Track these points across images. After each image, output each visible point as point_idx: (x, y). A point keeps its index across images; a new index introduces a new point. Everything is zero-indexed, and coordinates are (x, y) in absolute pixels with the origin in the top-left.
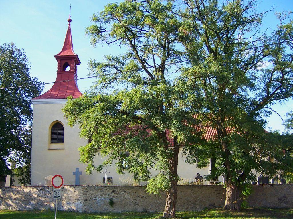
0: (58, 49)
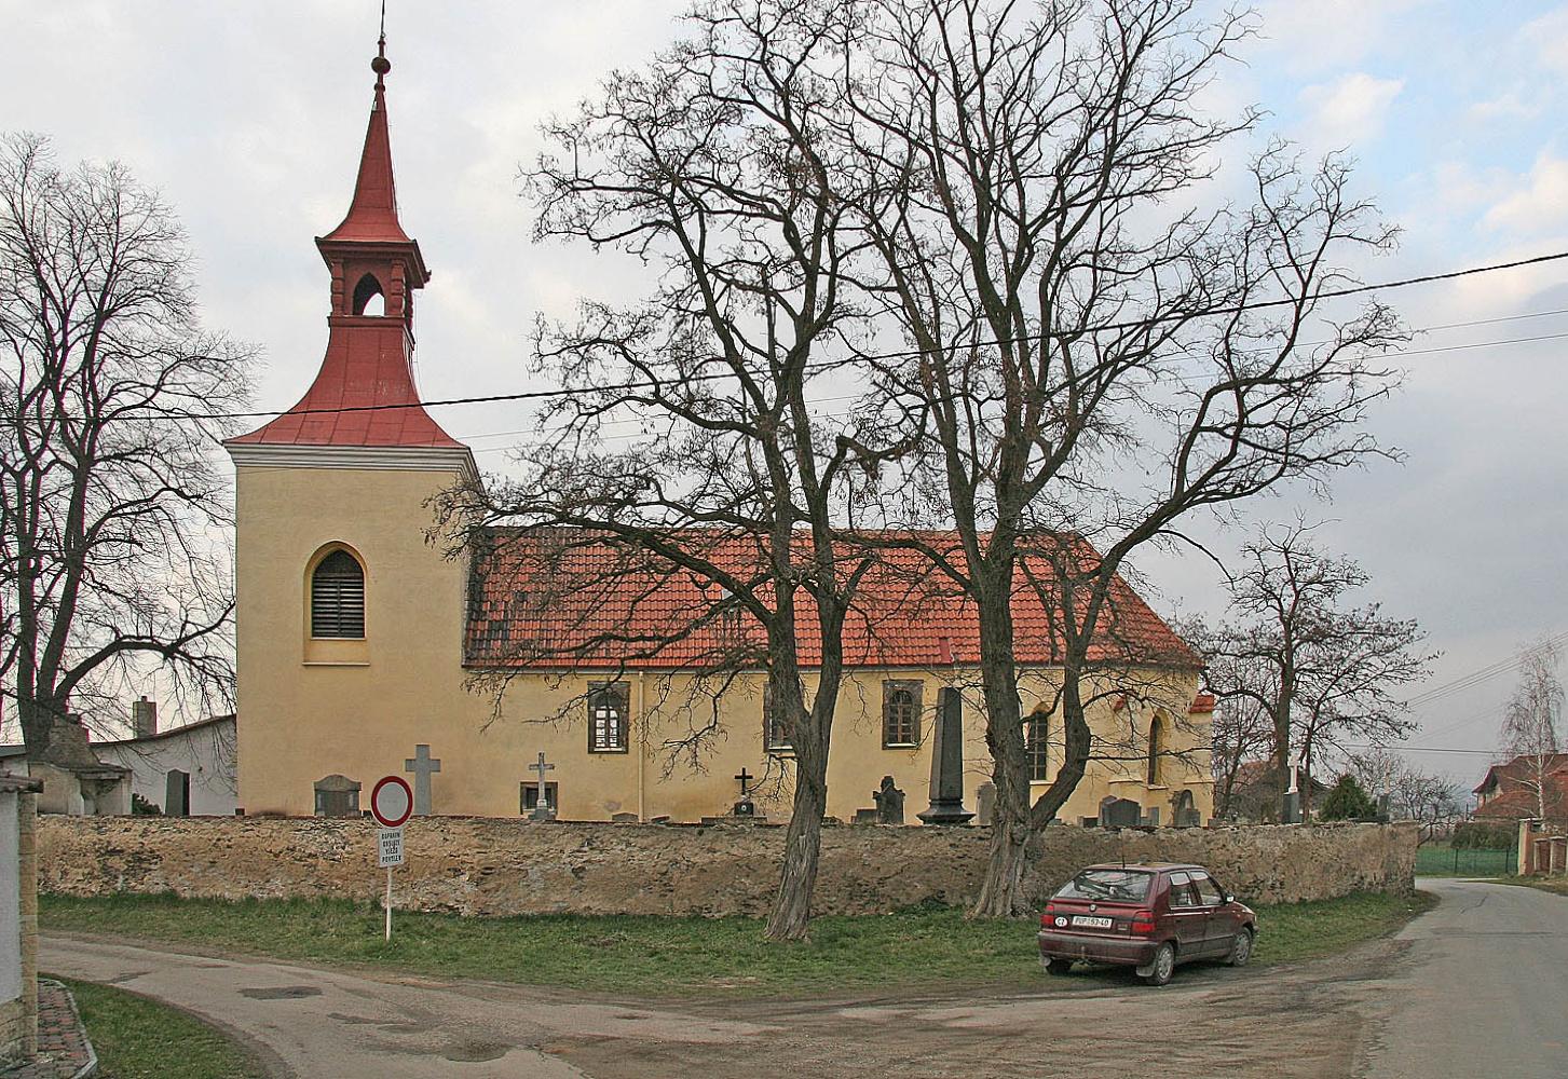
0: (331, 211)
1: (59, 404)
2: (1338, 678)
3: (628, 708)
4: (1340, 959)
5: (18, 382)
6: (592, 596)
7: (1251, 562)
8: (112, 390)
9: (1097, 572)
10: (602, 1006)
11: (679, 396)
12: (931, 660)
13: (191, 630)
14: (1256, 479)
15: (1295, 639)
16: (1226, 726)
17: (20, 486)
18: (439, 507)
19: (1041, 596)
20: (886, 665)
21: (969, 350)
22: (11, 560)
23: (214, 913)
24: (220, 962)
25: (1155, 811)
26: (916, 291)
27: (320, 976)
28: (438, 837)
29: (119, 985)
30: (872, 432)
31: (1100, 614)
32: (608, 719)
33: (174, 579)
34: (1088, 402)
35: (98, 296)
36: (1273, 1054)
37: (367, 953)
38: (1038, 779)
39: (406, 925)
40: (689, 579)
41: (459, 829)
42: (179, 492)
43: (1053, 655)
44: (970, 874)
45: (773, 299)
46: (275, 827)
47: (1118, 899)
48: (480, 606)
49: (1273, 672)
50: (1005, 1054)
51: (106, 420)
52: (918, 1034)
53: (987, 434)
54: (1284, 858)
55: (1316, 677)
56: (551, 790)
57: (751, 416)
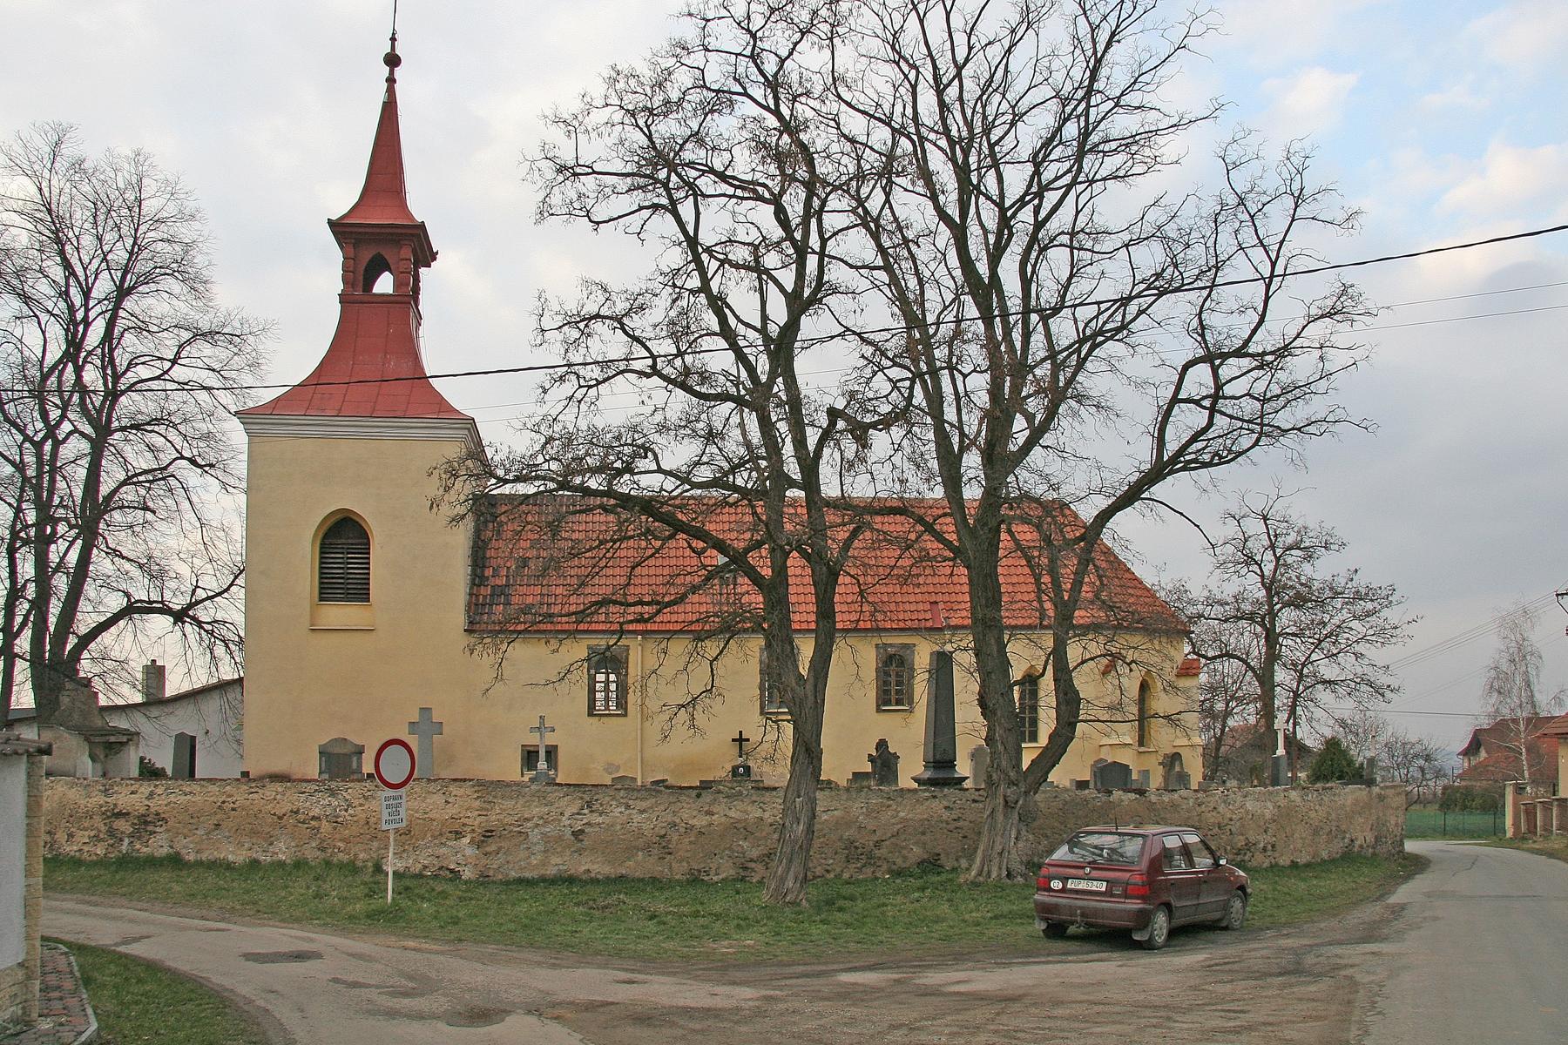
0: (344, 195)
1: (79, 377)
2: (1320, 641)
3: (627, 672)
4: (1334, 922)
5: (40, 355)
6: (591, 562)
7: (1231, 529)
8: (130, 364)
9: (1082, 538)
10: (601, 971)
11: (675, 369)
12: (923, 624)
13: (201, 594)
14: (1234, 448)
15: (1277, 603)
16: (1212, 689)
17: (39, 455)
18: (444, 476)
19: (1029, 561)
20: (879, 630)
21: (953, 326)
22: (28, 526)
23: (218, 876)
24: (222, 925)
25: (1145, 774)
26: (901, 269)
27: (323, 940)
28: (439, 799)
29: (122, 949)
30: (862, 404)
31: (1086, 580)
32: (607, 682)
33: (186, 545)
34: (1069, 375)
35: (119, 274)
36: (1271, 1019)
37: (368, 917)
38: (1030, 741)
39: (407, 888)
40: (686, 545)
41: (461, 792)
42: (193, 461)
43: (1041, 619)
44: (965, 837)
45: (765, 277)
46: (280, 790)
47: (1108, 863)
48: (483, 572)
49: (1257, 636)
50: (1004, 1019)
51: (123, 393)
52: (917, 999)
53: (972, 405)
54: (1275, 821)
55: (1298, 640)
56: (551, 752)
57: (745, 388)
